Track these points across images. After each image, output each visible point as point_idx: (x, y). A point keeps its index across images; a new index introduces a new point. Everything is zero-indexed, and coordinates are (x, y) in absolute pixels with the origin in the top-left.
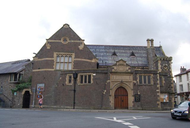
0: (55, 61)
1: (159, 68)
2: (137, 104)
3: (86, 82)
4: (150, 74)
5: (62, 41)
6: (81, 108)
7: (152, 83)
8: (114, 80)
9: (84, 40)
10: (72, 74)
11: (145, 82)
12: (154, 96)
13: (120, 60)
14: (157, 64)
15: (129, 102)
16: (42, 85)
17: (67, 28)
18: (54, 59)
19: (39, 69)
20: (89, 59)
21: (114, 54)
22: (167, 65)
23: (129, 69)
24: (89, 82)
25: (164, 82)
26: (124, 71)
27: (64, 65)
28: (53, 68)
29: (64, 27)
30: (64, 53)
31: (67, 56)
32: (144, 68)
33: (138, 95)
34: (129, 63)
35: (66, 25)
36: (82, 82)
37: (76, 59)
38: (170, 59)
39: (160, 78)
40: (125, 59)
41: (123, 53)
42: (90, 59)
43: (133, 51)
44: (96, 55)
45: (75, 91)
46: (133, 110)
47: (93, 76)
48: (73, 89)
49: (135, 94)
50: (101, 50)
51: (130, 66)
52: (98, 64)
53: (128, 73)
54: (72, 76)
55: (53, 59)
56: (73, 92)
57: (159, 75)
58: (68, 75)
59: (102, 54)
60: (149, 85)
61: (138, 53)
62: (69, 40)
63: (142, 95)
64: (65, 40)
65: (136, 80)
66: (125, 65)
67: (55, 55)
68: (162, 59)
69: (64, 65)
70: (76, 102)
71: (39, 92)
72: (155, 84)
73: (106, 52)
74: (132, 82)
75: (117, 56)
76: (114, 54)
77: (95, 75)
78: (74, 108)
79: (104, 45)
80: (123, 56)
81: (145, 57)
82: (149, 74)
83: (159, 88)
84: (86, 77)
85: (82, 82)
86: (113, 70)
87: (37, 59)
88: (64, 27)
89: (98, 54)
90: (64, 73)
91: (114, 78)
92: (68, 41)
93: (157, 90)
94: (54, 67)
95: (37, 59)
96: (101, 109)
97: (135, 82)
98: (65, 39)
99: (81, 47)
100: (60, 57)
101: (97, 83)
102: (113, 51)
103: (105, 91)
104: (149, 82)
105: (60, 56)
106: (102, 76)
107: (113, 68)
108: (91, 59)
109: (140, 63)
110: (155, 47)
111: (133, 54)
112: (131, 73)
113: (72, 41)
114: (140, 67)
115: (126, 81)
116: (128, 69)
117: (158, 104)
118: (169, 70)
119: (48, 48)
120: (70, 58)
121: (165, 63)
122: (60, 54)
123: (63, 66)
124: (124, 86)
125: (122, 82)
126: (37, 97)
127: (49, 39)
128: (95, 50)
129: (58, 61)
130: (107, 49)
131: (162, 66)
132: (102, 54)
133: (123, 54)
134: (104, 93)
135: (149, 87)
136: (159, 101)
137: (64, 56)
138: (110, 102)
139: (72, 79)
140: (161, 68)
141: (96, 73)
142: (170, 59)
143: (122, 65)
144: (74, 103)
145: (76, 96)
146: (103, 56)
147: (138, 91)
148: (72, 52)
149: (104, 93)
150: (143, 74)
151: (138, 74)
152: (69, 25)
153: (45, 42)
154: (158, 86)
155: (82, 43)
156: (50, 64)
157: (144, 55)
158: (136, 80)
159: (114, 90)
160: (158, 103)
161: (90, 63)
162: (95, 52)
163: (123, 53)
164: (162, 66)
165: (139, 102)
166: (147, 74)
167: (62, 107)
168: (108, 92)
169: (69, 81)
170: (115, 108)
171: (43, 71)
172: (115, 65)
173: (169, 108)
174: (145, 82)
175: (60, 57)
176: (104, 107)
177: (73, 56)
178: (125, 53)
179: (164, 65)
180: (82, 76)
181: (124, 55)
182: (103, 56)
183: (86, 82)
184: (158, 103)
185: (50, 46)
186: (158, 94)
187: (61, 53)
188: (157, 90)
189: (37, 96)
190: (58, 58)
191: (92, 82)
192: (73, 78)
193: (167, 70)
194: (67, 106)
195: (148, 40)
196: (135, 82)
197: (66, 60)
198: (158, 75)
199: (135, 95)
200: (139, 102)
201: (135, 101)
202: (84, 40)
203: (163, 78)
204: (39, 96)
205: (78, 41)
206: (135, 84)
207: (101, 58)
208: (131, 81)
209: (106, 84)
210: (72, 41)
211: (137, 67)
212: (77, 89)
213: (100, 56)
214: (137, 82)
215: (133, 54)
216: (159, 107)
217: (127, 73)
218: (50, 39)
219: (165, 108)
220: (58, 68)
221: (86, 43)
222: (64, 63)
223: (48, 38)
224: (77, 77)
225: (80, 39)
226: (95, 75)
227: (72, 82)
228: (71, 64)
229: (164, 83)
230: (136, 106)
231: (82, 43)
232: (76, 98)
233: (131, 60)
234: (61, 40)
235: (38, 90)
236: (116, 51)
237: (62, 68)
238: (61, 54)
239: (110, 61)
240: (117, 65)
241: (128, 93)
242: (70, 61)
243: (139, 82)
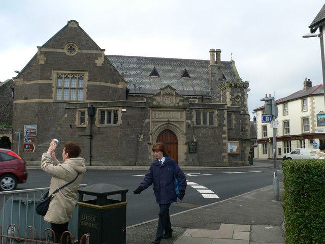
0: (54, 85)
1: (228, 100)
3: (109, 122)
5: (65, 51)
6: (103, 164)
7: (216, 124)
8: (157, 120)
9: (104, 50)
10: (86, 109)
11: (205, 122)
13: (166, 87)
14: (225, 93)
15: (179, 154)
16: (33, 128)
17: (75, 28)
18: (53, 82)
19: (26, 99)
20: (113, 83)
21: (155, 73)
22: (240, 94)
23: (181, 101)
24: (115, 122)
25: (234, 122)
26: (173, 104)
27: (77, 94)
28: (52, 98)
30: (69, 72)
31: (76, 78)
32: (204, 97)
34: (179, 89)
35: (74, 22)
37: (91, 83)
38: (246, 85)
39: (229, 116)
40: (174, 83)
41: (169, 71)
42: (115, 83)
43: (185, 68)
44: (123, 73)
46: (185, 166)
47: (123, 112)
48: (89, 134)
50: (132, 66)
52: (127, 91)
53: (180, 107)
54: (86, 113)
55: (50, 82)
57: (226, 111)
58: (78, 109)
59: (133, 73)
60: (210, 126)
61: (194, 72)
62: (79, 49)
63: (200, 143)
64: (71, 49)
65: (191, 119)
66: (175, 94)
67: (54, 75)
68: (233, 85)
69: (77, 94)
70: (94, 154)
71: (28, 139)
72: (220, 125)
73: (140, 69)
74: (185, 123)
75: (159, 76)
76: (155, 73)
77: (125, 110)
78: (91, 165)
79: (136, 57)
80: (169, 77)
81: (207, 80)
83: (227, 131)
84: (109, 113)
85: (102, 122)
86: (155, 103)
87: (20, 82)
88: (70, 25)
89: (126, 72)
90: (73, 107)
91: (157, 115)
92: (77, 51)
93: (223, 135)
94: (53, 95)
95: (20, 82)
96: (135, 165)
97: (189, 122)
98: (71, 47)
99: (99, 62)
100: (63, 79)
101: (128, 125)
102: (152, 67)
103: (142, 137)
104: (211, 123)
105: (63, 76)
106: (136, 113)
107: (155, 100)
108: (117, 82)
109: (198, 89)
110: (224, 63)
111: (186, 74)
112: (184, 108)
113: (85, 51)
114: (198, 97)
115: (175, 120)
116: (178, 101)
117: (224, 157)
118: (243, 103)
119: (42, 62)
120: (81, 81)
121: (238, 92)
122: (62, 74)
123: (75, 95)
124: (172, 128)
125: (169, 122)
126: (25, 147)
127: (43, 46)
128: (121, 65)
129: (60, 85)
130: (142, 64)
132: (133, 73)
133: (168, 74)
134: (140, 140)
136: (226, 152)
137: (70, 76)
139: (87, 116)
140: (231, 100)
141: (127, 107)
142: (246, 85)
143: (170, 95)
144: (91, 156)
145: (94, 144)
146: (135, 76)
147: (194, 137)
148: (84, 71)
152: (77, 23)
153: (36, 51)
154: (225, 129)
155: (100, 55)
156: (46, 91)
157: (204, 76)
158: (191, 119)
159: (157, 134)
160: (224, 154)
161: (115, 90)
162: (122, 69)
163: (169, 71)
164: (233, 97)
168: (146, 138)
169: (81, 120)
171: (33, 103)
172: (159, 94)
173: (240, 162)
174: (205, 122)
175: (63, 79)
176: (140, 162)
177: (86, 77)
178: (172, 71)
179: (235, 94)
180: (103, 113)
181: (172, 74)
182: (135, 76)
183: (109, 122)
184: (224, 154)
185: (46, 58)
186: (224, 141)
187: (65, 72)
188: (223, 135)
189: (25, 146)
190: (60, 80)
191: (120, 122)
193: (241, 103)
195: (212, 51)
196: (189, 122)
197: (74, 85)
198: (226, 112)
199: (189, 142)
200: (195, 154)
201: (189, 153)
202: (104, 50)
203: (233, 117)
204: (27, 146)
205: (95, 52)
206: (188, 126)
207: (132, 79)
208: (181, 120)
209: (144, 125)
210: (85, 51)
211: (192, 97)
213: (130, 76)
214: (193, 122)
215: (186, 74)
216: (226, 160)
217: (177, 108)
220: (59, 98)
221: (106, 53)
222: (71, 90)
223: (41, 45)
224: (94, 113)
225: (97, 48)
226: (125, 110)
227: (87, 122)
228: (82, 90)
230: (190, 160)
231: (100, 55)
232: (94, 149)
233: (182, 85)
234: (63, 49)
235: (25, 135)
236: (158, 67)
237: (66, 99)
238: (65, 74)
239: (149, 85)
240: (162, 94)
241: (179, 139)
242: (81, 86)
243: (195, 123)
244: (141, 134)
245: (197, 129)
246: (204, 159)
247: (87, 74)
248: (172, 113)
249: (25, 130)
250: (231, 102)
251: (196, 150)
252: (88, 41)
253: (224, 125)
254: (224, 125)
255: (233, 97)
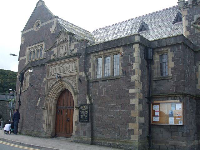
0: (26, 60)
2: (83, 127)
4: (117, 49)
12: (123, 108)
17: (41, 6)
23: (76, 46)
25: (172, 65)
29: (38, 6)
33: (87, 105)
49: (80, 103)
51: (78, 41)
63: (96, 106)
77: (31, 71)
82: (114, 50)
86: (52, 57)
93: (131, 91)
97: (83, 74)
107: (52, 53)
113: (44, 24)
117: (131, 131)
127: (24, 30)
131: (190, 22)
135: (113, 82)
136: (134, 122)
138: (44, 121)
143: (64, 41)
149: (38, 105)
150: (102, 53)
151: (92, 56)
154: (135, 78)
160: (131, 126)
164: (192, 23)
165: (87, 122)
166: (110, 51)
170: (55, 135)
184: (131, 126)
188: (131, 91)
198: (136, 47)
199: (81, 105)
201: (80, 121)
210: (44, 24)
218: (24, 30)
219: (171, 142)
226: (31, 71)
229: (172, 69)
231: (53, 23)
244: (39, 97)
245: (94, 84)
246: (101, 132)
248: (67, 65)
250: (188, 32)
251: (88, 119)
252: (47, 14)
253: (133, 72)
254: (133, 72)
255: (192, 23)
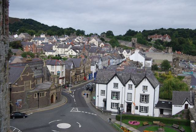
3: (42, 96)
7: (59, 91)
16: (20, 100)
36: (41, 96)
45: (38, 100)
56: (38, 101)
84: (42, 93)
85: (41, 96)
167: (33, 108)
183: (42, 96)
192: (37, 95)
194: (35, 107)
210: (30, 74)
212: (39, 100)
247: (31, 81)
249: (17, 101)
